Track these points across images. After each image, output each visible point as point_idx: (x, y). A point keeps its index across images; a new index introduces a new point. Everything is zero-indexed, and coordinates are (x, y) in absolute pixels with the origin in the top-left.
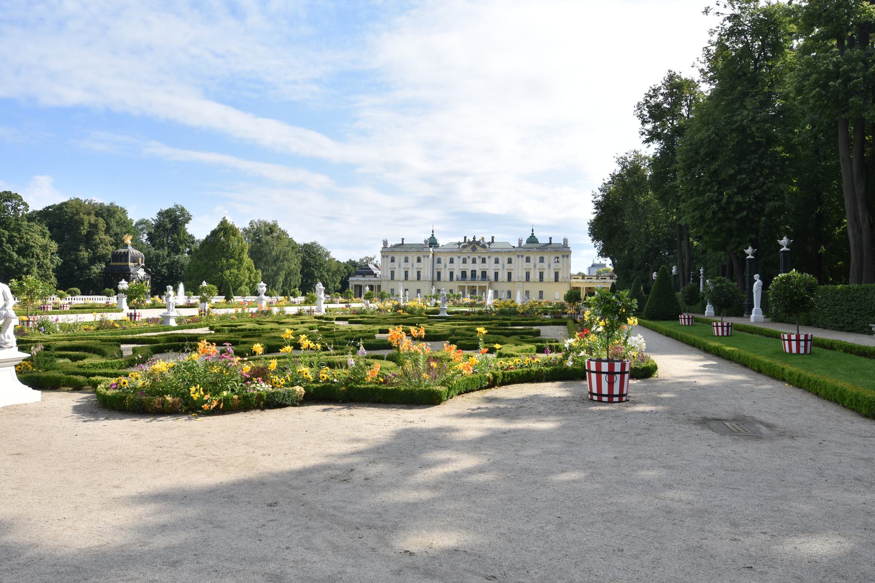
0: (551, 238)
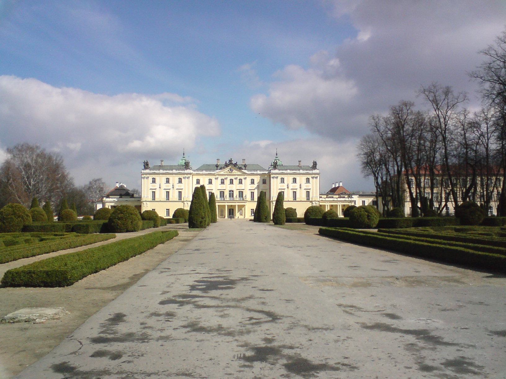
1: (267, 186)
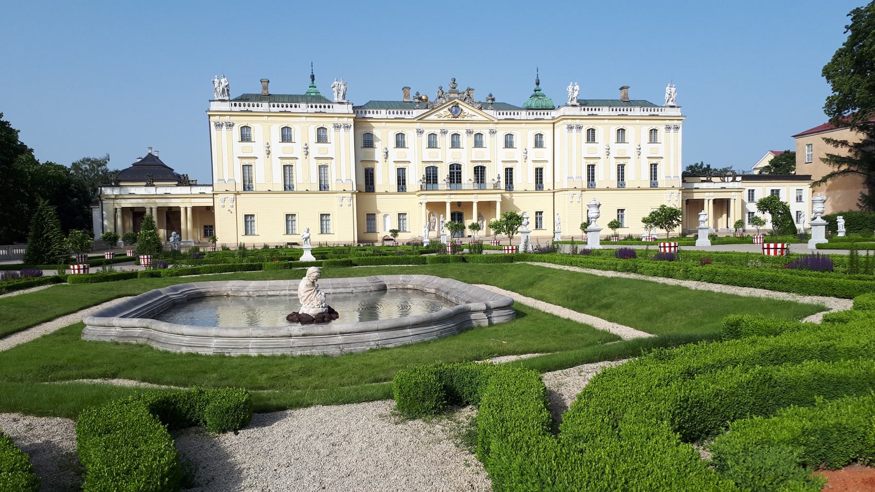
1: (545, 153)
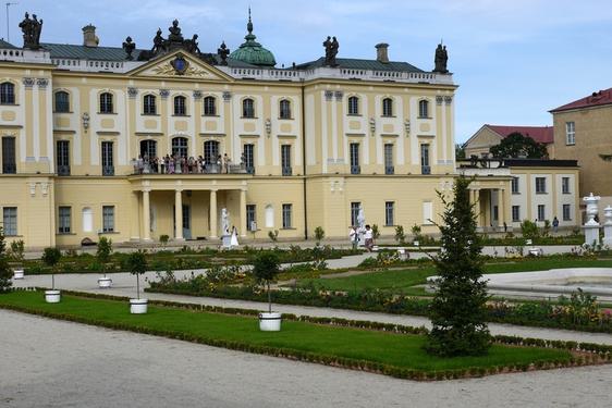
0: (382, 47)
1: (294, 126)
